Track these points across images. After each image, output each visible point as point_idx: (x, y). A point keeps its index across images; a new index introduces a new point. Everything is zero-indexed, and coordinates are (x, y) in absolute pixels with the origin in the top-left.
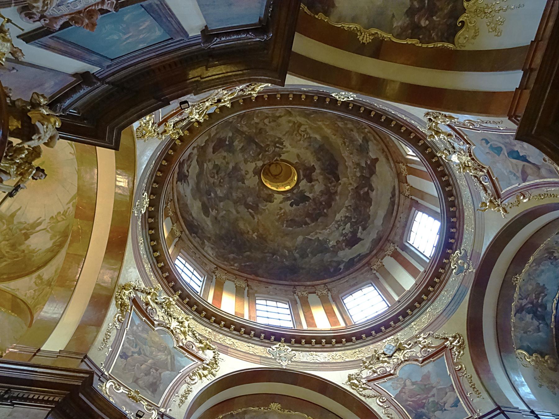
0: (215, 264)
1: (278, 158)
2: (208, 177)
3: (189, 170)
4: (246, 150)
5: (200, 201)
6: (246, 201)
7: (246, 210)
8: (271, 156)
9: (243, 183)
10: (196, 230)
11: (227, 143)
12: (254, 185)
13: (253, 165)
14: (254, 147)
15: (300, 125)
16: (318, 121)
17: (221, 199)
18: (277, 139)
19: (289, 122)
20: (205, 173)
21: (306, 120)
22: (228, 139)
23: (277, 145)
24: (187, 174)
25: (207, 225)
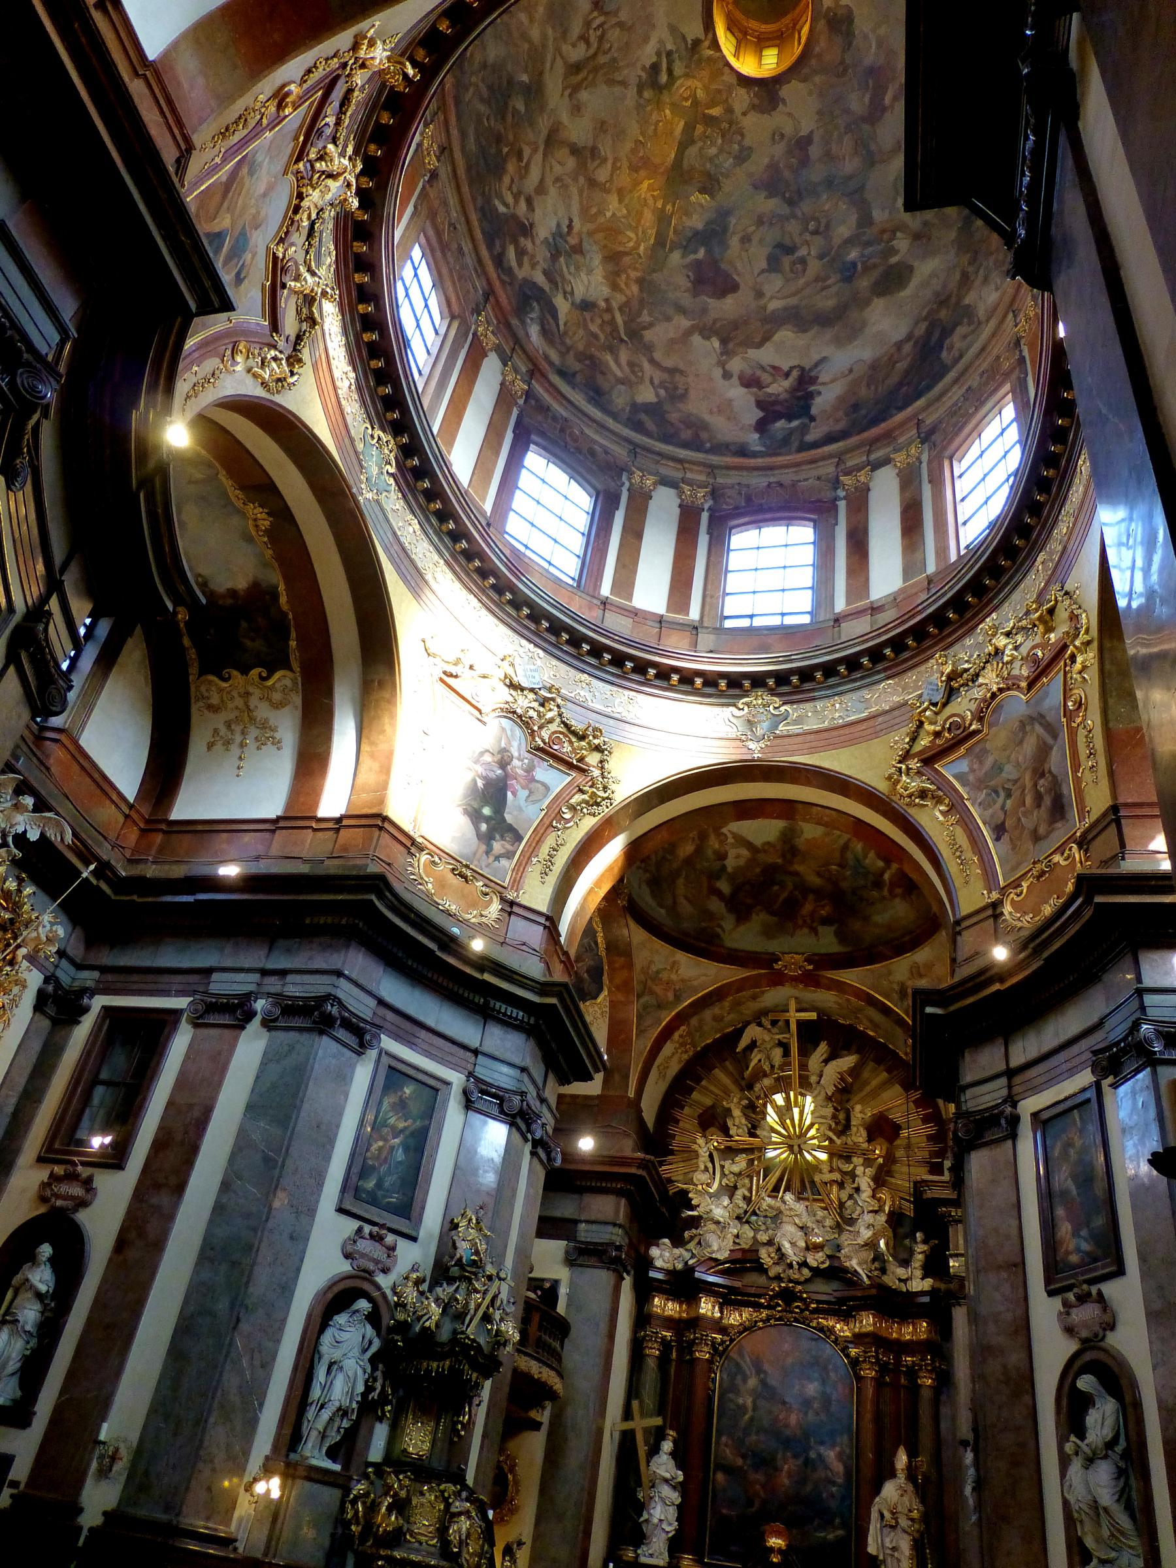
0: (1005, 316)
1: (707, 43)
2: (807, 284)
3: (786, 368)
4: (709, 175)
5: (868, 302)
6: (864, 119)
7: (888, 115)
8: (705, 74)
9: (808, 140)
10: (936, 335)
11: (701, 254)
12: (810, 93)
13: (751, 122)
14: (692, 151)
15: (575, 68)
16: (530, 42)
17: (865, 220)
18: (647, 94)
19: (577, 109)
20: (793, 301)
21: (547, 75)
22: (692, 257)
23: (664, 78)
24: (795, 374)
25: (931, 276)
